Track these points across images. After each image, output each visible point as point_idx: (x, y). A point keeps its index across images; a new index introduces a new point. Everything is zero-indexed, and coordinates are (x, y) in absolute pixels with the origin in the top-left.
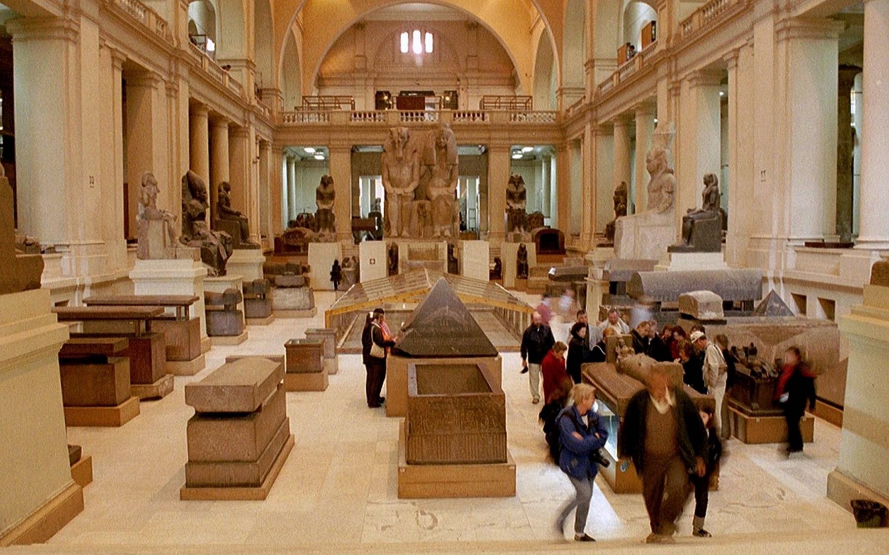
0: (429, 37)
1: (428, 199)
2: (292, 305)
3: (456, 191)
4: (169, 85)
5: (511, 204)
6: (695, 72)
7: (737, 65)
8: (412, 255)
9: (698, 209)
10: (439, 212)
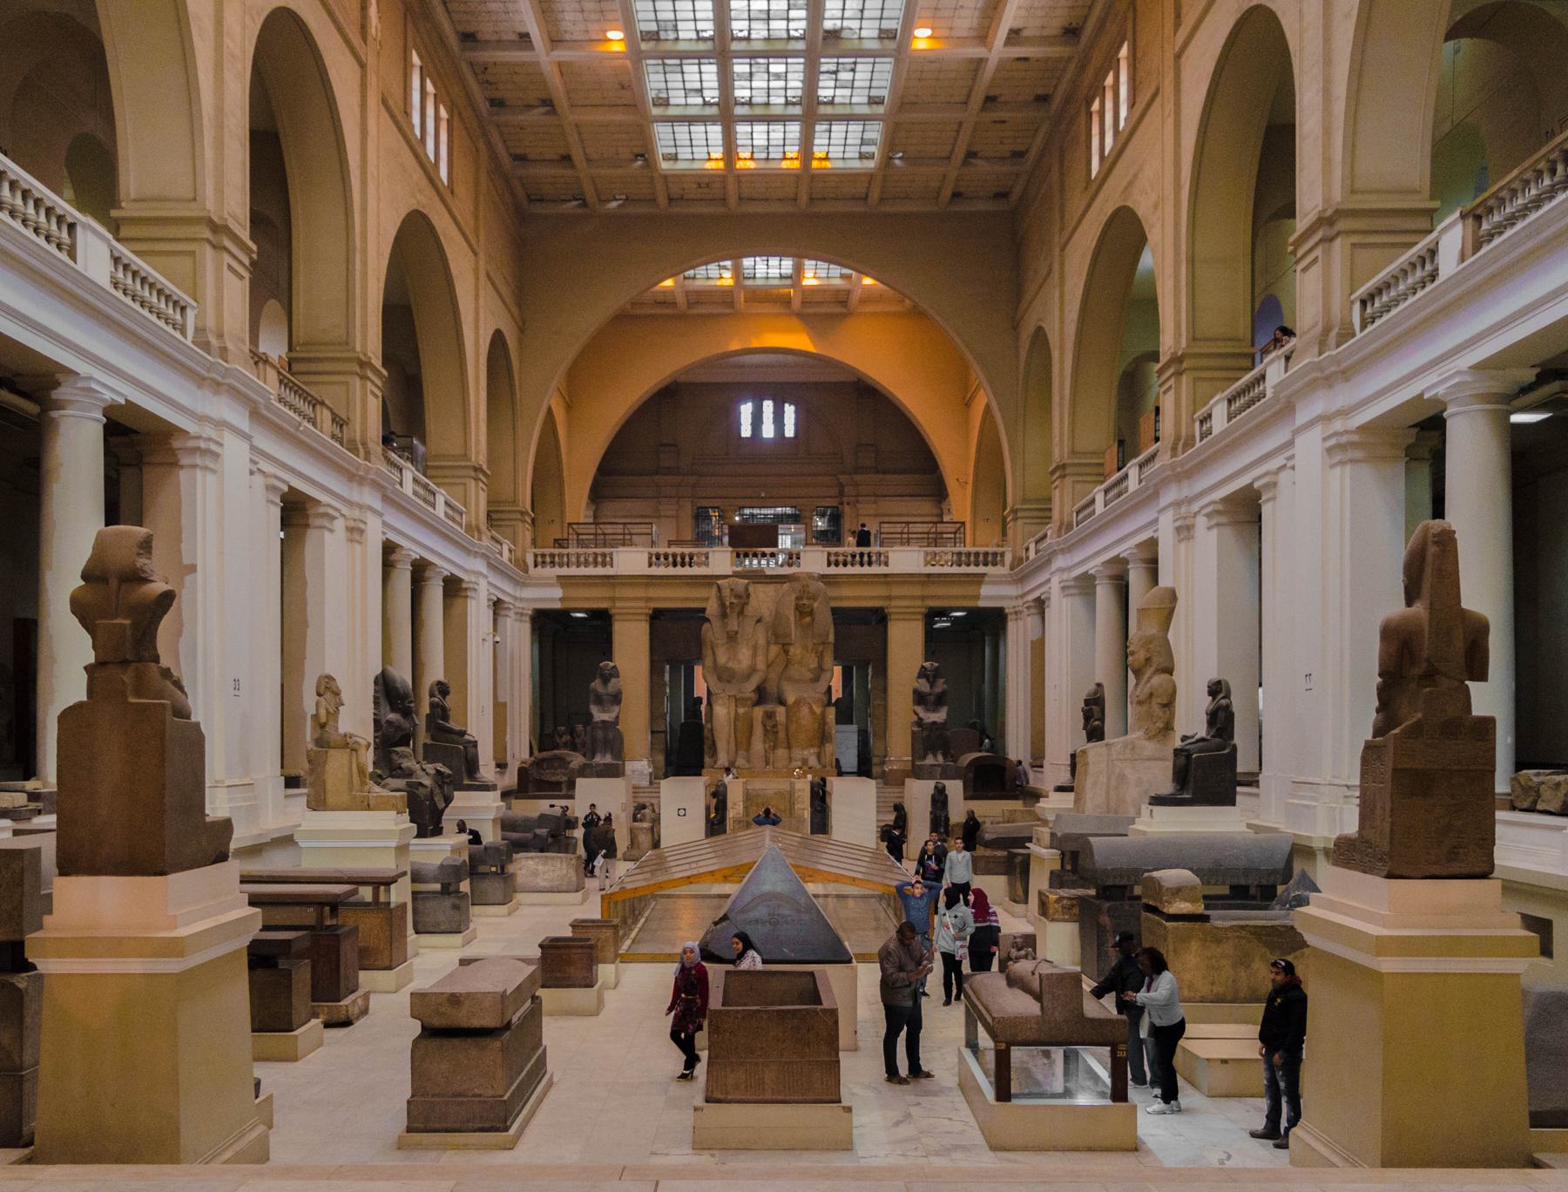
0: (790, 411)
1: (782, 702)
4: (352, 524)
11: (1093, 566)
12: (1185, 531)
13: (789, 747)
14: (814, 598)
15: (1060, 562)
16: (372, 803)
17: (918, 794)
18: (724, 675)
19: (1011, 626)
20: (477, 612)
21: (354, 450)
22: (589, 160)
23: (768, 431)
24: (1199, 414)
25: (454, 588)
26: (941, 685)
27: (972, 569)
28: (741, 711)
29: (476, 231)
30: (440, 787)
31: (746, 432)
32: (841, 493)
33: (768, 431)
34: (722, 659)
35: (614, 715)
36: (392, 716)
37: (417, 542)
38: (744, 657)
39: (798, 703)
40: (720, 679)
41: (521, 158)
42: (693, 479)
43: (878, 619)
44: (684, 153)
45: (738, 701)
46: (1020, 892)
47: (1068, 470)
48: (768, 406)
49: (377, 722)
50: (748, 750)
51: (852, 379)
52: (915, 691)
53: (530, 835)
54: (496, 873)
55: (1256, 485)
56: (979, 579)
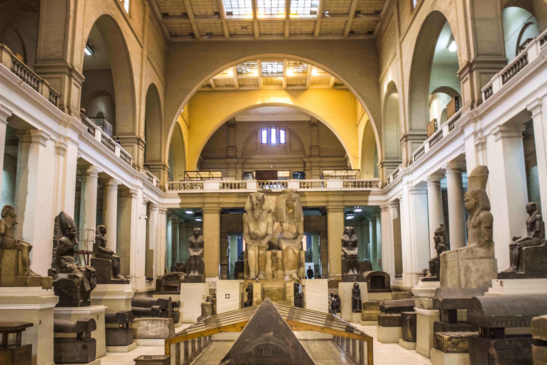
0: (282, 132)
1: (280, 249)
2: (153, 334)
3: (302, 242)
4: (58, 145)
5: (346, 251)
6: (499, 126)
7: (541, 113)
8: (264, 293)
9: (522, 238)
10: (288, 259)
11: (425, 178)
12: (481, 145)
13: (284, 269)
14: (294, 201)
15: (406, 179)
16: (28, 281)
17: (345, 289)
18: (255, 237)
19: (383, 214)
20: (137, 207)
21: (63, 110)
22: (195, 15)
23: (274, 141)
24: (484, 88)
25: (124, 193)
26: (354, 238)
27: (365, 189)
28: (261, 252)
29: (143, 38)
30: (89, 279)
31: (264, 141)
32: (305, 166)
33: (274, 141)
34: (252, 229)
35: (200, 253)
36: (63, 239)
37: (101, 163)
38: (262, 228)
39: (287, 248)
40: (251, 238)
41: (165, 15)
42: (242, 160)
43: (324, 211)
44: (235, 12)
45: (259, 248)
46: (410, 335)
47: (409, 138)
48: (273, 131)
49: (55, 242)
50: (264, 271)
51: (308, 119)
52: (343, 241)
53: (150, 309)
54: (122, 328)
55: (529, 109)
56: (368, 193)
